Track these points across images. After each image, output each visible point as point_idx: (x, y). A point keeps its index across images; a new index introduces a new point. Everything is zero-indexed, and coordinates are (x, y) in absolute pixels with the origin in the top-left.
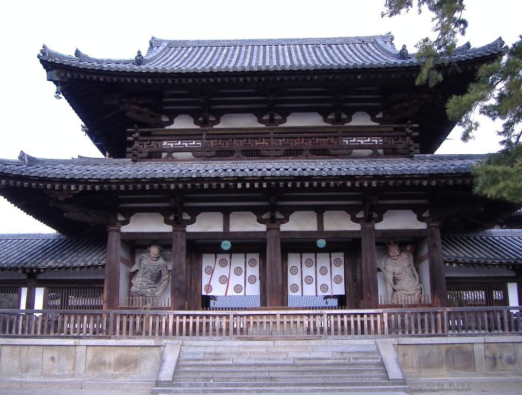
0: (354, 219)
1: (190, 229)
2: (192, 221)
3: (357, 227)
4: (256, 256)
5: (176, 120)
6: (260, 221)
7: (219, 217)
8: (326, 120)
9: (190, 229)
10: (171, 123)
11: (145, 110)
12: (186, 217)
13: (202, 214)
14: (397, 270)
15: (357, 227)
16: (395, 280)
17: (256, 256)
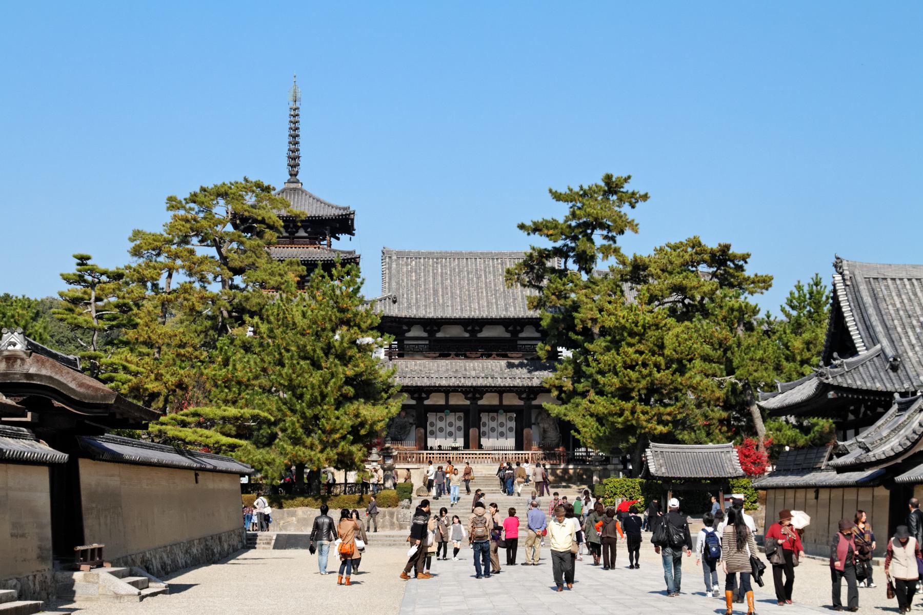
0: (520, 399)
1: (426, 402)
2: (427, 398)
3: (522, 403)
4: (462, 414)
5: (412, 329)
6: (467, 398)
7: (443, 395)
8: (507, 331)
9: (426, 402)
10: (409, 331)
11: (394, 324)
12: (424, 395)
13: (433, 394)
14: (546, 426)
15: (522, 403)
16: (545, 431)
17: (462, 414)
